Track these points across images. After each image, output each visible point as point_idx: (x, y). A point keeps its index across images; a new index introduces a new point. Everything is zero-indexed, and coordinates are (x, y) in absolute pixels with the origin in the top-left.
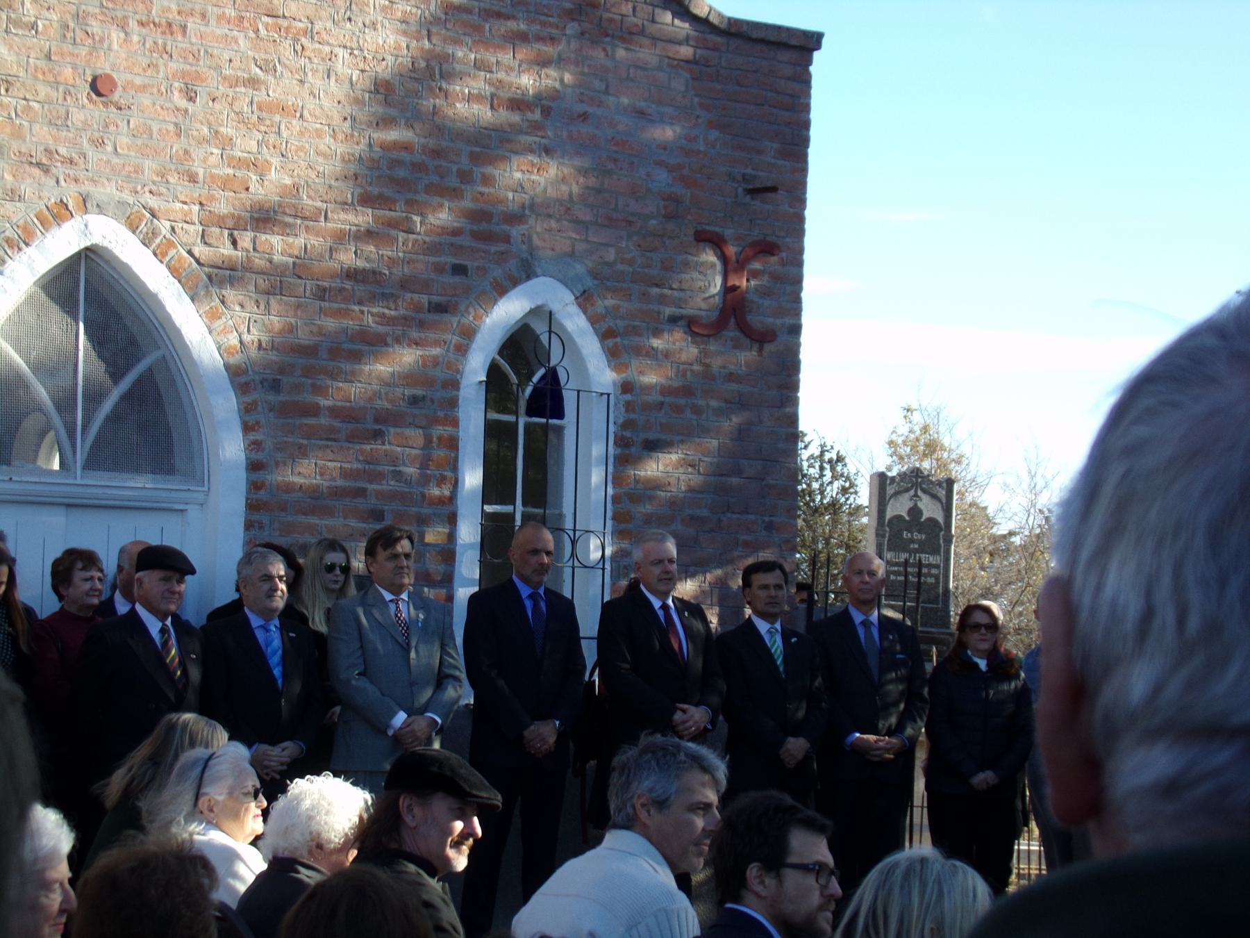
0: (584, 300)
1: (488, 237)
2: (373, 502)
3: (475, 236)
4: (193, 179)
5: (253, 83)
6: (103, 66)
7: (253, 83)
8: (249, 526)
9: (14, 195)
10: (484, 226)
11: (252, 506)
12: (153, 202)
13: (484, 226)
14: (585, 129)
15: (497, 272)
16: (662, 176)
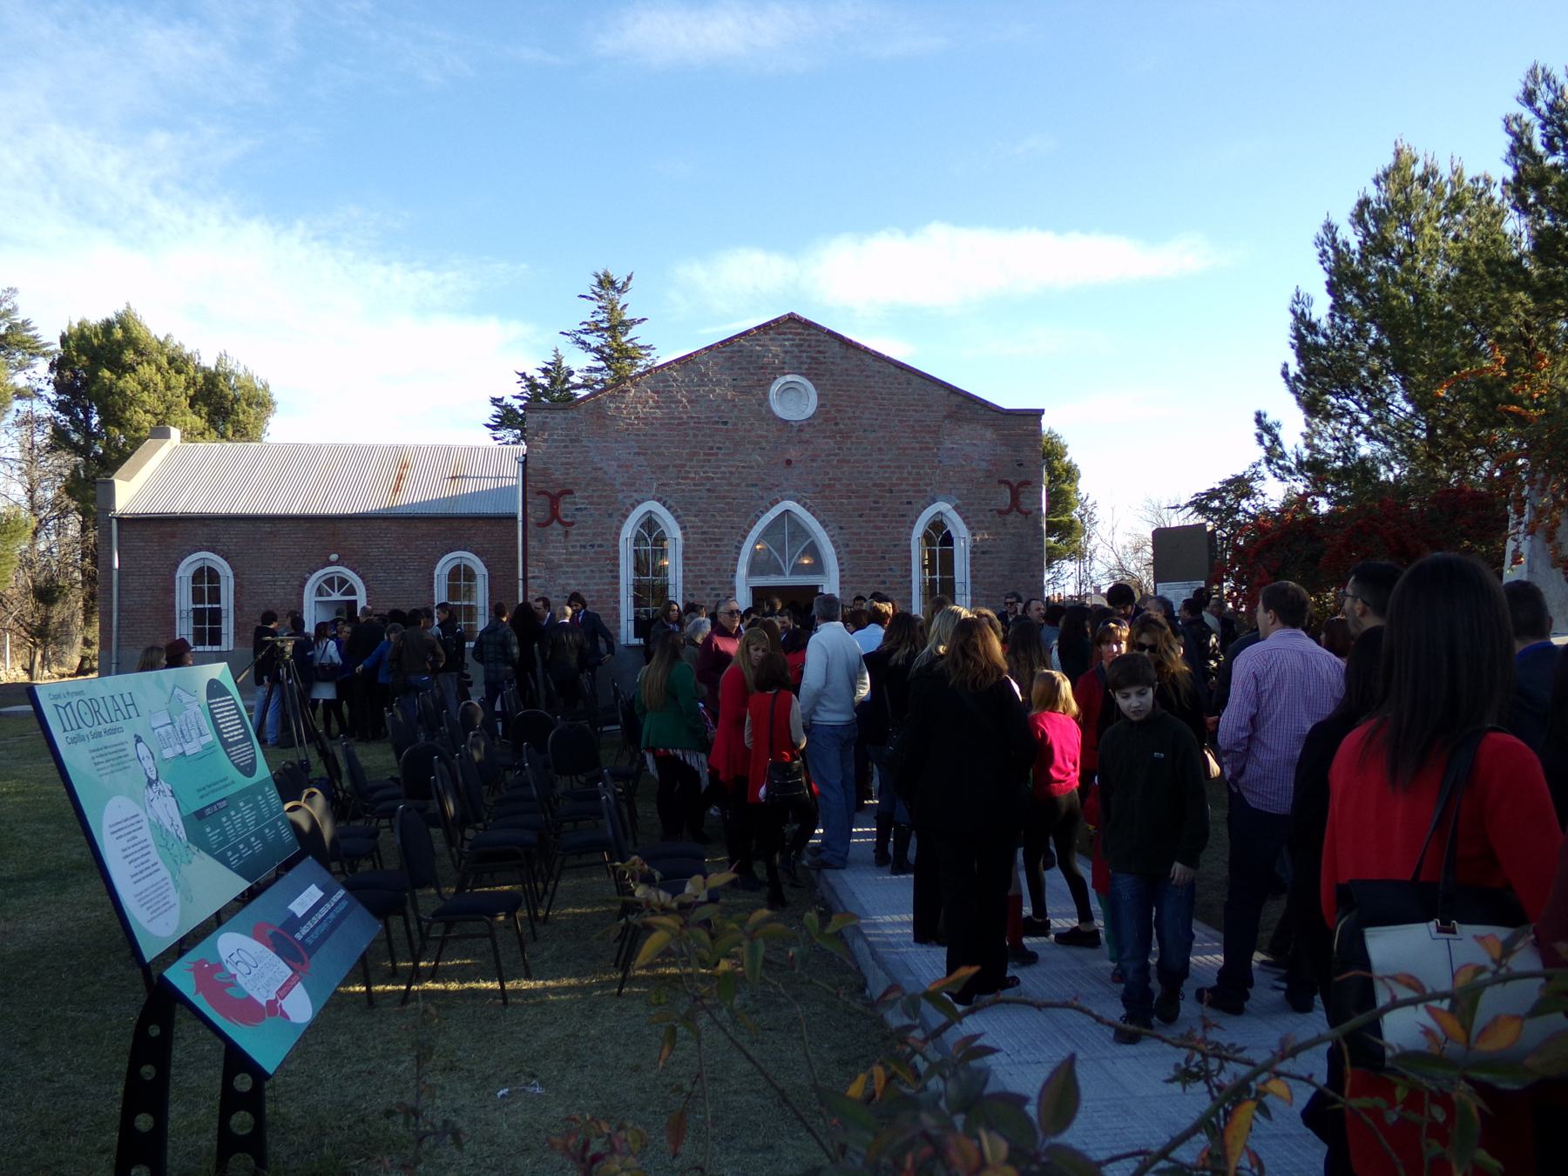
0: (956, 508)
1: (920, 491)
2: (882, 578)
3: (915, 491)
4: (817, 486)
5: (836, 455)
6: (788, 457)
7: (836, 455)
8: (841, 588)
9: (762, 498)
10: (917, 488)
11: (841, 582)
12: (805, 494)
13: (917, 488)
14: (953, 452)
15: (922, 502)
16: (984, 464)
